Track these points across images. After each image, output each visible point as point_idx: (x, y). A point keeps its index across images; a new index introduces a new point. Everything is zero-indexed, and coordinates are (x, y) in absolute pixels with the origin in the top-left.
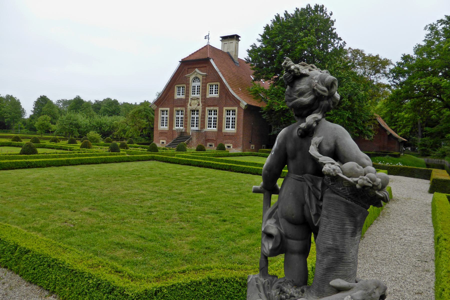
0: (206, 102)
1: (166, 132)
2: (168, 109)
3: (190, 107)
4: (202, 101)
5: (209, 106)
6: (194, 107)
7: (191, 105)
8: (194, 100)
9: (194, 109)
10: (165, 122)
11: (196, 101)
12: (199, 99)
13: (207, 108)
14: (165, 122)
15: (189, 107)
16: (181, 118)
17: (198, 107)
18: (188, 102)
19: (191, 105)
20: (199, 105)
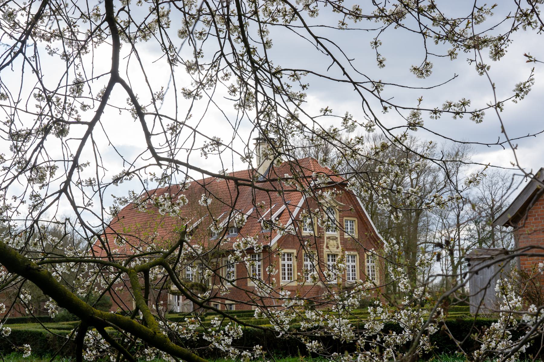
0: (346, 245)
1: (294, 289)
2: (295, 251)
3: (328, 250)
4: (341, 243)
5: (348, 250)
6: (334, 250)
7: (327, 247)
8: (333, 239)
9: (333, 253)
10: (286, 272)
11: (335, 242)
12: (337, 238)
13: (347, 253)
14: (286, 272)
15: (326, 251)
16: (288, 265)
17: (338, 250)
18: (324, 242)
19: (327, 247)
20: (338, 248)
